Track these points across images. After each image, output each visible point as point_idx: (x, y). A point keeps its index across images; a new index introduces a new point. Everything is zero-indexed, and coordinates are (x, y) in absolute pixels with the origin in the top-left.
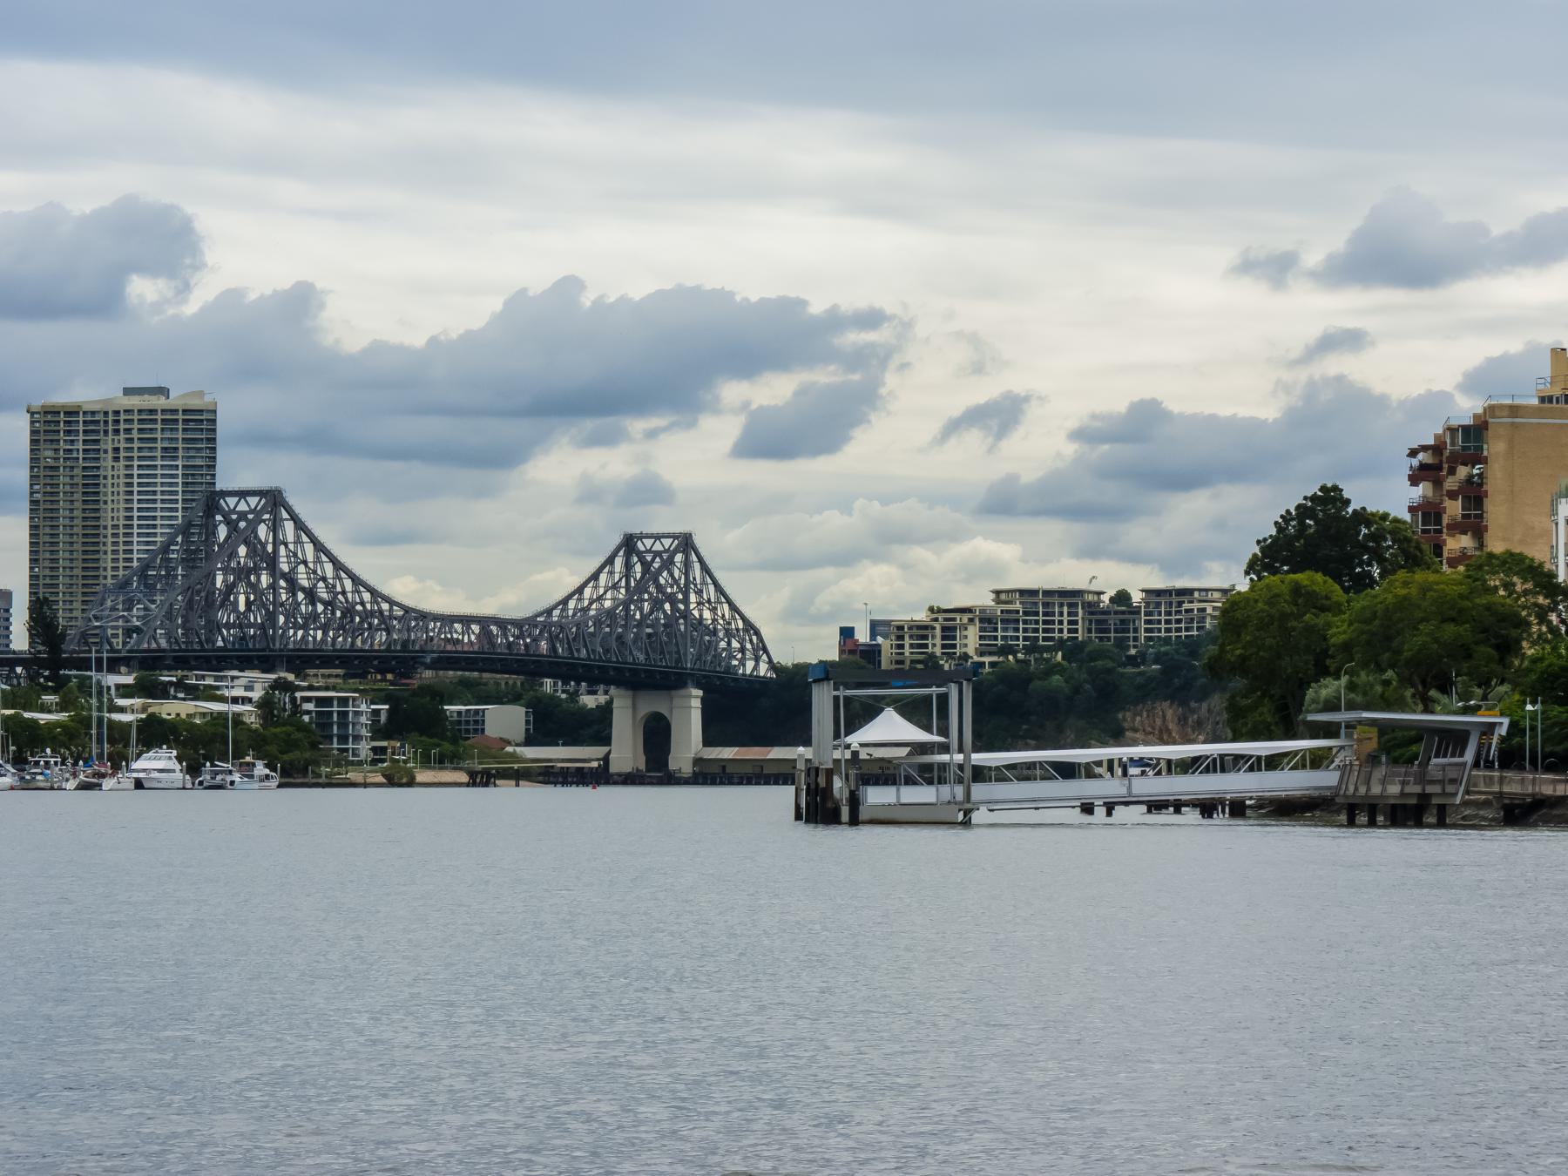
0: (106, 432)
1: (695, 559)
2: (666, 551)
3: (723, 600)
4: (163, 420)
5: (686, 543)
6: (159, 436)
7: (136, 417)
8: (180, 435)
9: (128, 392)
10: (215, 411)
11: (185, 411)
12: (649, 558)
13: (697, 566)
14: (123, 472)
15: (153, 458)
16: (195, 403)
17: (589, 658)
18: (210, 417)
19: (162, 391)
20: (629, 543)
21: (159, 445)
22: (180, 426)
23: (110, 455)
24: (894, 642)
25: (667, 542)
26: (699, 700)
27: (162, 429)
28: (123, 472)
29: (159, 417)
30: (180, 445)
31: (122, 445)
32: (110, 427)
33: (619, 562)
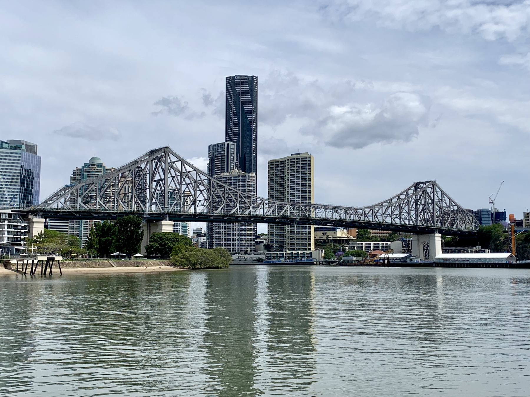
1: (438, 189)
3: (454, 204)
4: (296, 161)
5: (433, 184)
6: (295, 166)
8: (301, 165)
9: (292, 155)
10: (310, 158)
11: (302, 158)
13: (440, 194)
15: (294, 172)
17: (413, 225)
18: (309, 159)
19: (299, 154)
20: (416, 186)
21: (295, 168)
22: (301, 163)
24: (526, 219)
25: (427, 184)
26: (440, 238)
27: (297, 164)
29: (295, 160)
30: (301, 168)
33: (411, 192)
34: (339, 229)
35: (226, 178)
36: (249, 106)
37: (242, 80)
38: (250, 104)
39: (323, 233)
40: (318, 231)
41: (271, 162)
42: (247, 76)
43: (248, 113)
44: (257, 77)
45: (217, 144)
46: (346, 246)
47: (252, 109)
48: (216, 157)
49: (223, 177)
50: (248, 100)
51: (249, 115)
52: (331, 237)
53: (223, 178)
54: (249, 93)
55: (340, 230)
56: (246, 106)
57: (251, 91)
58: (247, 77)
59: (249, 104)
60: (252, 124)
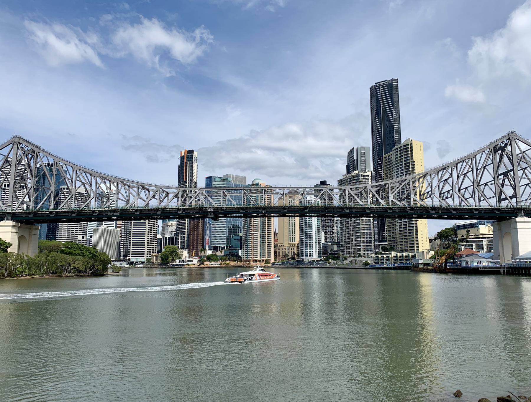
34: (484, 224)
36: (389, 109)
37: (381, 86)
38: (391, 107)
39: (467, 231)
40: (462, 229)
42: (386, 81)
43: (389, 116)
44: (397, 79)
45: (351, 150)
46: (463, 245)
47: (392, 111)
48: (350, 163)
50: (389, 103)
51: (391, 118)
52: (473, 236)
54: (388, 96)
55: (485, 226)
56: (387, 110)
57: (391, 94)
58: (386, 82)
59: (389, 107)
60: (393, 126)
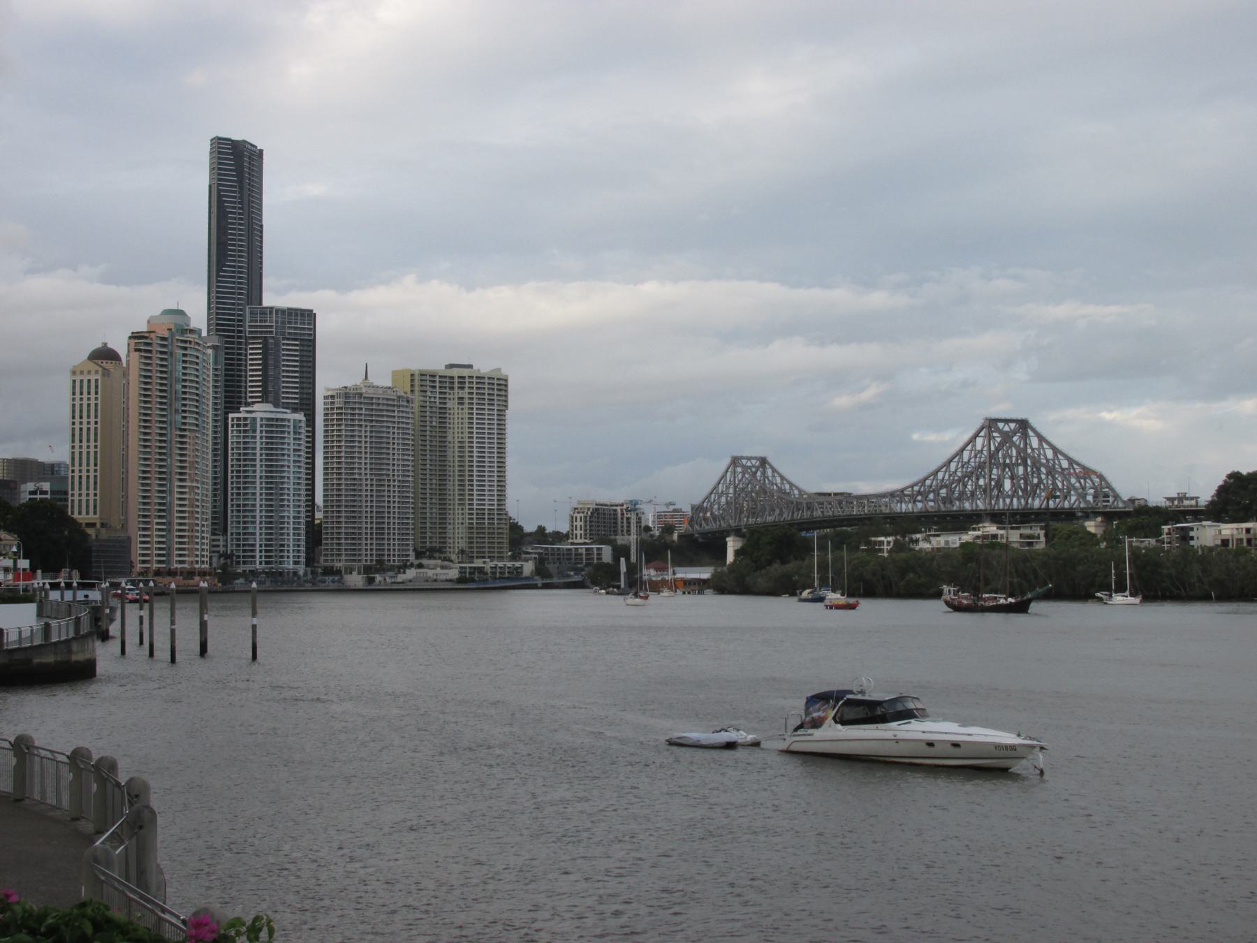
0: (452, 388)
2: (754, 466)
5: (764, 462)
7: (475, 380)
9: (452, 366)
10: (506, 380)
12: (754, 469)
14: (467, 411)
16: (496, 375)
19: (470, 366)
20: (735, 461)
23: (456, 401)
25: (754, 462)
28: (467, 411)
31: (467, 396)
32: (456, 385)
35: (372, 398)
41: (422, 375)
48: (284, 339)
49: (364, 395)
53: (365, 398)
